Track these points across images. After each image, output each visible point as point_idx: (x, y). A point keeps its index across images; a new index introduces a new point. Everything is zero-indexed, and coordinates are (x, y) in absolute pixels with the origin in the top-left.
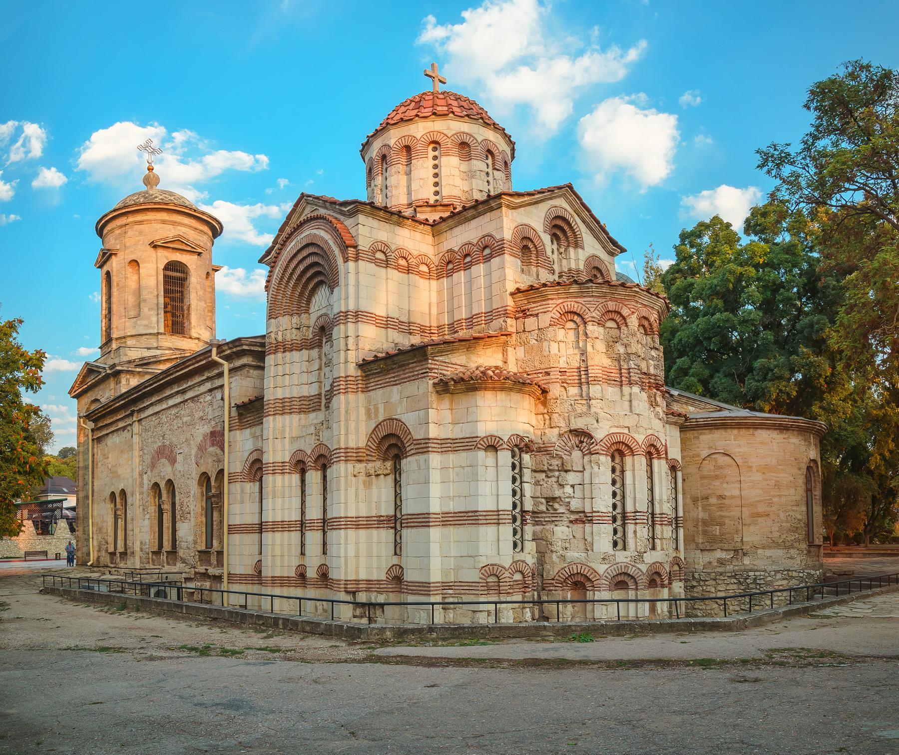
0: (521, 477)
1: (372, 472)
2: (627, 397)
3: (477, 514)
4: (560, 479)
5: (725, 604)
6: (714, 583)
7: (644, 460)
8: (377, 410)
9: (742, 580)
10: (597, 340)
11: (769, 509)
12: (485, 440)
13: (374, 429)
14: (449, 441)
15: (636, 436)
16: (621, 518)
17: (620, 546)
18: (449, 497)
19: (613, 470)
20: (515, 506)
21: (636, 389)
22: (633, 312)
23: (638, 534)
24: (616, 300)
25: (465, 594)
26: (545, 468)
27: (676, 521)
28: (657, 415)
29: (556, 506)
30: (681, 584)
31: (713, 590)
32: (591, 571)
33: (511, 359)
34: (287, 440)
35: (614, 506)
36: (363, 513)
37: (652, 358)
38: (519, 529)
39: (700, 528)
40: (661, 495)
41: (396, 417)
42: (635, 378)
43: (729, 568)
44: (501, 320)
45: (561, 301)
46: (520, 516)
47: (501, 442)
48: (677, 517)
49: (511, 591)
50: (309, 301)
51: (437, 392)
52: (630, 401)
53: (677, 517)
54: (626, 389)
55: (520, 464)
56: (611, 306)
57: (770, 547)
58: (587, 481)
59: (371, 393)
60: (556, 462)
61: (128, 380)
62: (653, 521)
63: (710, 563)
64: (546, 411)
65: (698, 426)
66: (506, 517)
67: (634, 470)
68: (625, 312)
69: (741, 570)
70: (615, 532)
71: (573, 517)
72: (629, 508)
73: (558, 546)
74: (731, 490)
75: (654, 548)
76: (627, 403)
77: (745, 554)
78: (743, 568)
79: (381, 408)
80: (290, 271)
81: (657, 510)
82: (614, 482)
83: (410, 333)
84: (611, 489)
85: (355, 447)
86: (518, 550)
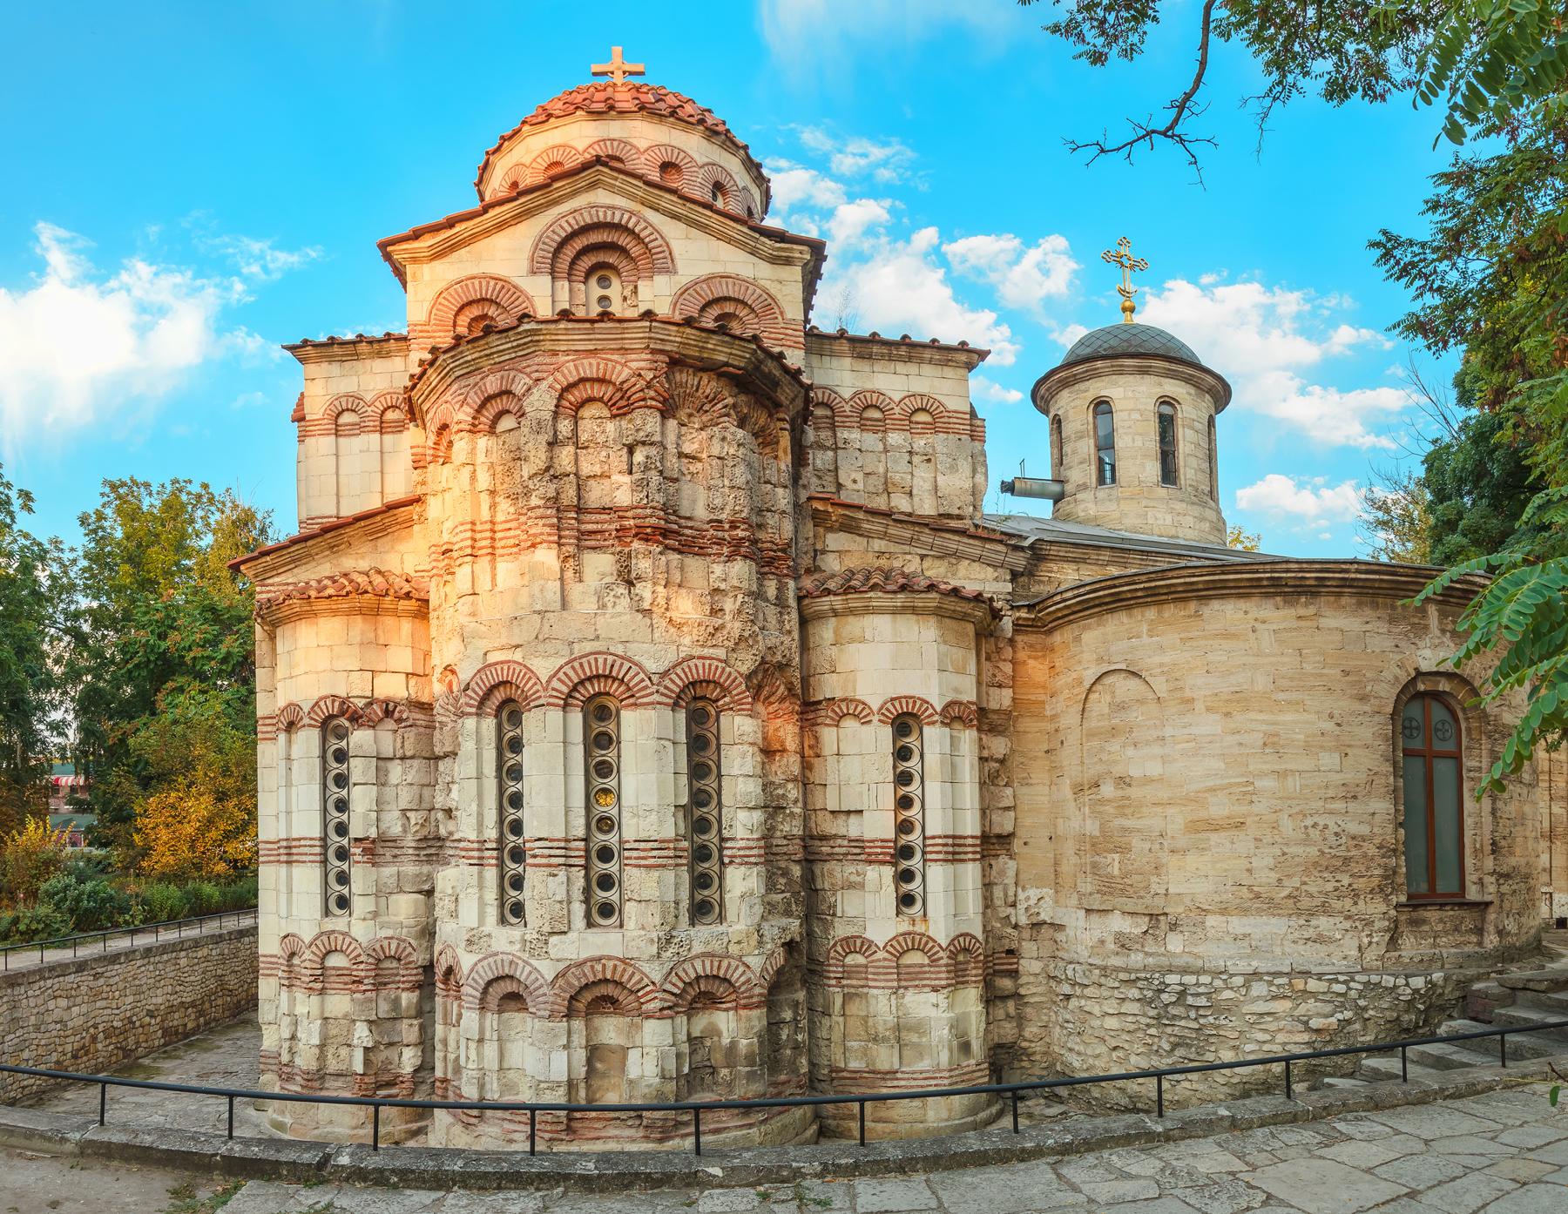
11: (1242, 809)
16: (510, 852)
43: (1136, 959)
49: (319, 986)
57: (1244, 911)
66: (306, 850)
77: (1173, 927)
78: (1164, 961)
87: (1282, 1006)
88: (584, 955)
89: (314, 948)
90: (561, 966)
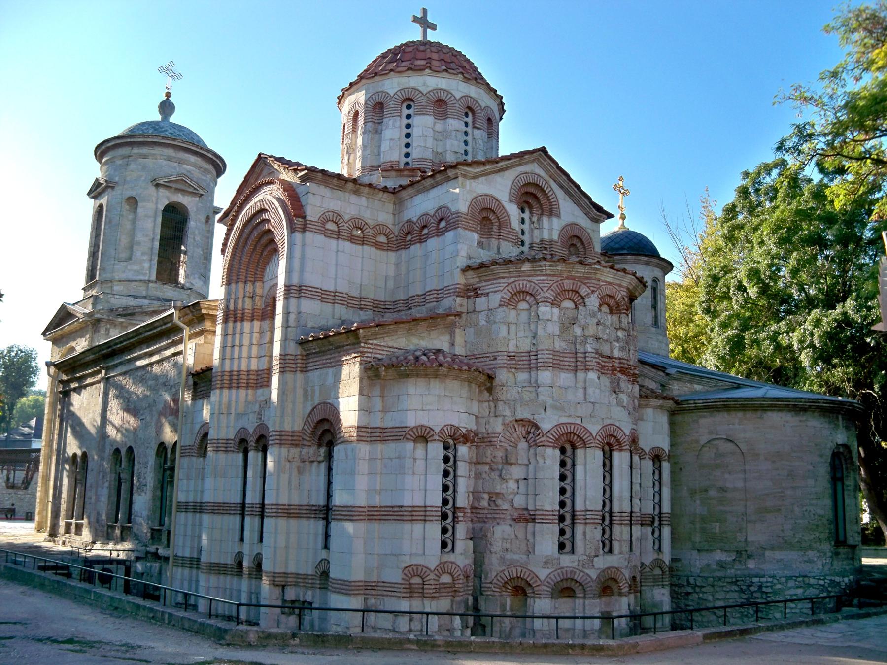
0: (455, 471)
1: (306, 458)
2: (580, 384)
3: (402, 509)
4: (504, 472)
5: (725, 615)
6: (711, 589)
7: (599, 454)
8: (313, 392)
9: (744, 587)
10: (549, 323)
12: (415, 430)
13: (310, 413)
14: (379, 430)
15: (590, 427)
16: (566, 517)
17: (568, 548)
18: (375, 490)
19: (563, 464)
20: (445, 502)
21: (592, 376)
22: (593, 292)
23: (587, 536)
24: (573, 278)
25: (387, 595)
26: (488, 460)
27: (660, 517)
28: (620, 404)
29: (499, 502)
30: (666, 591)
31: (710, 598)
32: (532, 575)
33: (459, 340)
34: (232, 416)
35: (562, 504)
36: (296, 501)
37: (618, 339)
38: (450, 528)
39: (698, 525)
40: (621, 491)
41: (329, 401)
42: (592, 362)
43: (731, 572)
44: (451, 299)
45: (512, 280)
46: (448, 514)
47: (432, 433)
48: (660, 513)
49: (437, 595)
50: (264, 269)
51: (369, 377)
52: (585, 388)
53: (660, 513)
54: (581, 375)
55: (455, 457)
56: (568, 284)
58: (531, 476)
59: (310, 374)
60: (500, 454)
61: (108, 330)
62: (611, 520)
63: (708, 565)
64: (491, 398)
65: (697, 408)
66: (433, 513)
67: (585, 464)
68: (584, 291)
69: (745, 576)
70: (562, 532)
71: (516, 515)
72: (579, 506)
73: (497, 546)
74: (734, 481)
75: (610, 551)
76: (581, 391)
77: (749, 557)
78: (746, 572)
79: (317, 389)
80: (245, 236)
81: (616, 508)
82: (563, 478)
83: (361, 309)
84: (557, 485)
85: (290, 430)
86: (447, 550)
87: (800, 591)
88: (606, 566)
89: (436, 572)
90: (599, 572)
